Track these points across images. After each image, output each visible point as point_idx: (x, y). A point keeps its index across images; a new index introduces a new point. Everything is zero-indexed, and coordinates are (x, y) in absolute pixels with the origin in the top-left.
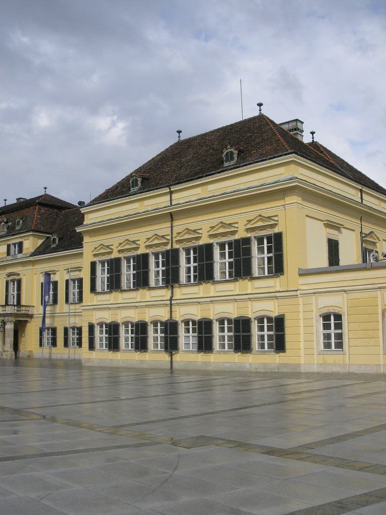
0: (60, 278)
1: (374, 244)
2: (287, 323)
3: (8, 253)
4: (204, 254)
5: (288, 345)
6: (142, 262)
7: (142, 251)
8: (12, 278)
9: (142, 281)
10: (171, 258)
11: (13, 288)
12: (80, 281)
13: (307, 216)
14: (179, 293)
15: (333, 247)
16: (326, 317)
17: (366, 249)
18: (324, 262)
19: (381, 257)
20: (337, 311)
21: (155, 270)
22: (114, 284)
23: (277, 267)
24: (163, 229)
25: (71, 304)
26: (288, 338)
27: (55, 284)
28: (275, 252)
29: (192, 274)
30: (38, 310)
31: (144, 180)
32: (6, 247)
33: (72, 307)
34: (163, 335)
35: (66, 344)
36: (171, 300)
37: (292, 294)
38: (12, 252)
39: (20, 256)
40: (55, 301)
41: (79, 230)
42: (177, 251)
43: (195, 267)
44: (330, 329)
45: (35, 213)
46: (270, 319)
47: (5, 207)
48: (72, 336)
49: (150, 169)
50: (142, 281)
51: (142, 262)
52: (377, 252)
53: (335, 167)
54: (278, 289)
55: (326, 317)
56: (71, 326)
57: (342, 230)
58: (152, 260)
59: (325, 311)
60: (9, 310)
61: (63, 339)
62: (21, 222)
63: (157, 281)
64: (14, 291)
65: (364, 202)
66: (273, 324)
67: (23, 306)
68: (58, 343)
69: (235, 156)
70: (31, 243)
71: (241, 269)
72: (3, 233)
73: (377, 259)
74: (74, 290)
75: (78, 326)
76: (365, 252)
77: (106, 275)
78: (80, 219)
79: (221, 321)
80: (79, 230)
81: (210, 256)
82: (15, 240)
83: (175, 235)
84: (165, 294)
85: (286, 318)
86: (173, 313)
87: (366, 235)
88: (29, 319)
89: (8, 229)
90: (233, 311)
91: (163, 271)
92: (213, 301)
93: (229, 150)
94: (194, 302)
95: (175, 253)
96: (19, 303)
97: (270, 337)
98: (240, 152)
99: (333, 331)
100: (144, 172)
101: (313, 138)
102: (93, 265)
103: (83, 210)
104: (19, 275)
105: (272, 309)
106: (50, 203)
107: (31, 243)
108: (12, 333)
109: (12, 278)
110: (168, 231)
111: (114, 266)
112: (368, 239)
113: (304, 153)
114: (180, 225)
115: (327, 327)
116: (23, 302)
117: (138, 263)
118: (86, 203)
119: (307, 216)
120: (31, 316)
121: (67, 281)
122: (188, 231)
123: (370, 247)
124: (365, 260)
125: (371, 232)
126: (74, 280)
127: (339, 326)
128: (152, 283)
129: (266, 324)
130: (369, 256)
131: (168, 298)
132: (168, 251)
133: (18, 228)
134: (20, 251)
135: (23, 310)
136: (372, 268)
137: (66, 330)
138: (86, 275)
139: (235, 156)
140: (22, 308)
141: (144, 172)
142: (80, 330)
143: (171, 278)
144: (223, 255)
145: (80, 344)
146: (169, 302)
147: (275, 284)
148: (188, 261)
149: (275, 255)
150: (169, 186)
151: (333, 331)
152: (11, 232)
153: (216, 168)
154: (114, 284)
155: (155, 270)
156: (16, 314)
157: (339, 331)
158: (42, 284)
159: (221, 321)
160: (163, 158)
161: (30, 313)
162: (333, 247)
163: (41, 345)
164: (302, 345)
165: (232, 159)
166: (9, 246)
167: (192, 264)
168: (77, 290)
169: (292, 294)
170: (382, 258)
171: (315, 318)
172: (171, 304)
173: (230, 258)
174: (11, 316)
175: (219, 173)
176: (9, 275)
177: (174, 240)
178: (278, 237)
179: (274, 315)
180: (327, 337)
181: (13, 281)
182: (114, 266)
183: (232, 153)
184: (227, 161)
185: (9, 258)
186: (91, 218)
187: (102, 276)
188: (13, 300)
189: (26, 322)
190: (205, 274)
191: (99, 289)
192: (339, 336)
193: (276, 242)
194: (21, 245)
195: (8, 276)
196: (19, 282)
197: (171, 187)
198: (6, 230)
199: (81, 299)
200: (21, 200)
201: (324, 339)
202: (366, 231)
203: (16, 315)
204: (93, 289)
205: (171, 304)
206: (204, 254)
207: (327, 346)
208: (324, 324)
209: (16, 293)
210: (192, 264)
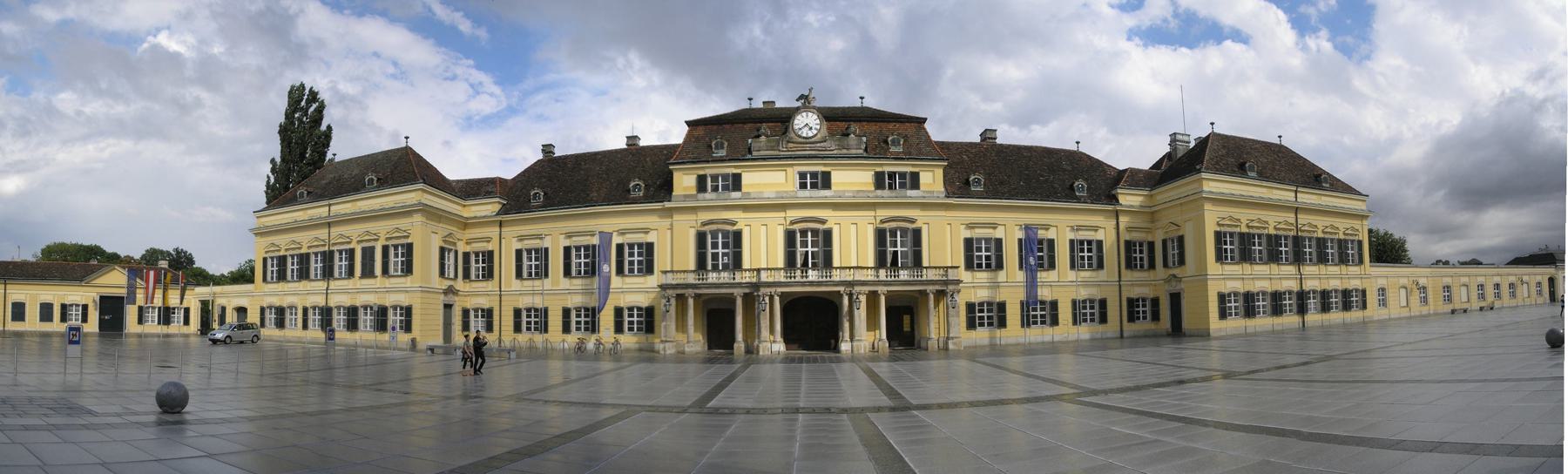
7: (304, 250)
10: (328, 257)
14: (334, 284)
21: (316, 266)
24: (322, 233)
42: (332, 253)
51: (304, 260)
58: (313, 258)
84: (322, 285)
94: (346, 292)
95: (332, 253)
110: (325, 236)
114: (335, 231)
122: (342, 236)
143: (328, 273)
147: (407, 282)
155: (316, 266)
179: (406, 304)
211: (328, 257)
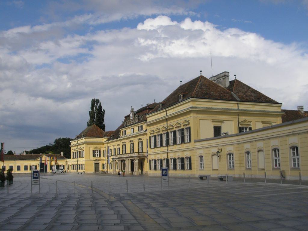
3: (138, 131)
32: (137, 127)
38: (140, 130)
39: (142, 131)
48: (179, 163)
62: (142, 117)
72: (136, 122)
88: (145, 158)
89: (138, 120)
96: (142, 152)
101: (235, 78)
104: (142, 139)
109: (140, 140)
133: (141, 119)
152: (139, 121)
163: (150, 169)
166: (138, 127)
174: (137, 157)
176: (139, 139)
181: (140, 142)
185: (139, 132)
189: (144, 159)
195: (139, 140)
198: (137, 120)
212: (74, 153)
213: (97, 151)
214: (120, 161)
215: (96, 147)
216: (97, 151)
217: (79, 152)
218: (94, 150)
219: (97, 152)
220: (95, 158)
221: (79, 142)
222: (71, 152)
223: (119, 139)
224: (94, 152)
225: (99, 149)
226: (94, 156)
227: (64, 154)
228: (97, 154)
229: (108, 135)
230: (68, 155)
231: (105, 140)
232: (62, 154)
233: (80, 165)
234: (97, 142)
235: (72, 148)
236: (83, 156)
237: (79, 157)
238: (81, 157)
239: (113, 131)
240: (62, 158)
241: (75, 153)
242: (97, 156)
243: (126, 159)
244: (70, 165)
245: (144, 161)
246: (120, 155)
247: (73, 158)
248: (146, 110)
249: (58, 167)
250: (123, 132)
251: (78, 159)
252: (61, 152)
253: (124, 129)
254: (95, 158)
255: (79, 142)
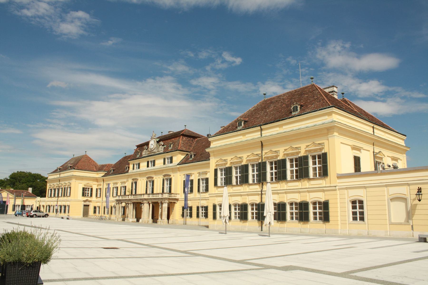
0: (195, 177)
1: (382, 158)
2: (330, 206)
4: (280, 165)
5: (331, 218)
6: (244, 169)
8: (167, 177)
9: (244, 180)
10: (261, 167)
11: (167, 183)
12: (207, 180)
13: (341, 143)
15: (357, 160)
16: (354, 202)
17: (377, 162)
18: (351, 169)
19: (386, 167)
20: (361, 198)
22: (228, 182)
23: (324, 172)
25: (202, 193)
26: (331, 214)
27: (192, 181)
28: (323, 163)
29: (274, 176)
30: (181, 196)
31: (245, 122)
33: (202, 194)
34: (257, 211)
35: (198, 216)
36: (262, 191)
37: (334, 189)
40: (192, 191)
41: (207, 150)
43: (276, 173)
44: (356, 209)
45: (181, 140)
46: (320, 203)
47: (162, 136)
49: (249, 115)
50: (244, 180)
52: (383, 164)
53: (357, 114)
54: (324, 185)
55: (354, 202)
56: (201, 205)
57: (362, 150)
59: (353, 198)
60: (166, 196)
61: (196, 213)
63: (254, 181)
64: (167, 185)
65: (375, 134)
66: (322, 206)
67: (173, 194)
68: (193, 215)
69: (299, 108)
70: (178, 157)
71: (302, 174)
73: (384, 169)
74: (203, 185)
75: (205, 205)
76: (376, 164)
77: (223, 177)
78: (208, 144)
79: (291, 204)
80: (207, 150)
81: (284, 166)
82: (168, 155)
83: (264, 154)
84: (257, 188)
85: (330, 202)
86: (263, 199)
87: (377, 153)
90: (298, 198)
91: (257, 174)
92: (287, 192)
93: (295, 105)
97: (320, 213)
98: (301, 106)
99: (358, 210)
100: (245, 117)
102: (216, 171)
103: (210, 139)
104: (170, 175)
105: (321, 197)
106: (188, 134)
107: (178, 157)
108: (166, 209)
109: (167, 177)
111: (228, 171)
112: (378, 155)
113: (339, 106)
115: (354, 207)
116: (173, 191)
117: (242, 170)
118: (212, 134)
119: (341, 143)
120: (177, 200)
121: (199, 180)
123: (379, 161)
124: (376, 168)
125: (380, 152)
126: (203, 179)
127: (362, 207)
128: (250, 181)
129: (317, 206)
130: (379, 166)
131: (260, 190)
132: (260, 163)
134: (171, 162)
135: (173, 197)
136: (382, 174)
137: (198, 208)
138: (211, 176)
139: (299, 108)
140: (172, 195)
141: (245, 117)
142: (206, 208)
143: (261, 179)
144: (292, 166)
145: (206, 216)
146: (260, 193)
148: (272, 169)
149: (323, 166)
150: (260, 126)
151: (358, 210)
153: (287, 115)
154: (228, 182)
155: (252, 174)
156: (169, 198)
157: (361, 210)
158: (184, 181)
159: (291, 204)
160: (256, 109)
161: (177, 198)
162: (357, 160)
164: (339, 218)
165: (297, 110)
167: (274, 171)
168: (204, 185)
169: (334, 189)
170: (387, 167)
171: (346, 202)
172: (262, 194)
173: (296, 167)
175: (289, 118)
177: (263, 157)
178: (325, 155)
180: (354, 213)
182: (228, 171)
183: (297, 107)
184: (294, 111)
186: (216, 144)
187: (221, 177)
188: (166, 190)
189: (174, 203)
190: (281, 176)
191: (219, 184)
192: (362, 213)
193: (323, 158)
194: (171, 158)
196: (171, 180)
197: (262, 127)
199: (207, 190)
200: (171, 133)
201: (353, 215)
202: (377, 151)
203: (169, 199)
204: (216, 184)
205: (262, 194)
206: (280, 165)
207: (355, 219)
208: (353, 206)
209: (168, 186)
210: (274, 171)
211: (261, 167)
212: (51, 190)
213: (89, 189)
214: (132, 205)
215: (88, 184)
216: (89, 189)
217: (62, 188)
218: (84, 187)
219: (88, 191)
220: (85, 199)
221: (62, 175)
222: (48, 188)
223: (127, 174)
224: (84, 189)
225: (91, 186)
226: (83, 195)
227: (33, 191)
228: (88, 193)
229: (104, 169)
230: (41, 192)
231: (100, 175)
232: (30, 190)
233: (61, 206)
234: (90, 177)
235: (48, 185)
236: (68, 195)
237: (60, 195)
238: (64, 196)
239: (112, 165)
240: (29, 196)
241: (53, 191)
242: (88, 195)
243: (145, 202)
244: (44, 206)
245: (174, 206)
246: (132, 196)
247: (49, 196)
248: (178, 138)
249: (23, 207)
250: (134, 165)
251: (60, 198)
252: (29, 188)
253: (137, 162)
254: (85, 199)
255: (62, 175)
